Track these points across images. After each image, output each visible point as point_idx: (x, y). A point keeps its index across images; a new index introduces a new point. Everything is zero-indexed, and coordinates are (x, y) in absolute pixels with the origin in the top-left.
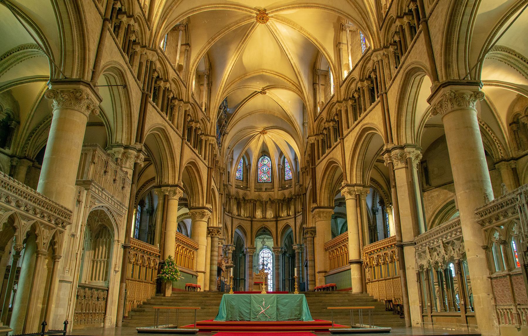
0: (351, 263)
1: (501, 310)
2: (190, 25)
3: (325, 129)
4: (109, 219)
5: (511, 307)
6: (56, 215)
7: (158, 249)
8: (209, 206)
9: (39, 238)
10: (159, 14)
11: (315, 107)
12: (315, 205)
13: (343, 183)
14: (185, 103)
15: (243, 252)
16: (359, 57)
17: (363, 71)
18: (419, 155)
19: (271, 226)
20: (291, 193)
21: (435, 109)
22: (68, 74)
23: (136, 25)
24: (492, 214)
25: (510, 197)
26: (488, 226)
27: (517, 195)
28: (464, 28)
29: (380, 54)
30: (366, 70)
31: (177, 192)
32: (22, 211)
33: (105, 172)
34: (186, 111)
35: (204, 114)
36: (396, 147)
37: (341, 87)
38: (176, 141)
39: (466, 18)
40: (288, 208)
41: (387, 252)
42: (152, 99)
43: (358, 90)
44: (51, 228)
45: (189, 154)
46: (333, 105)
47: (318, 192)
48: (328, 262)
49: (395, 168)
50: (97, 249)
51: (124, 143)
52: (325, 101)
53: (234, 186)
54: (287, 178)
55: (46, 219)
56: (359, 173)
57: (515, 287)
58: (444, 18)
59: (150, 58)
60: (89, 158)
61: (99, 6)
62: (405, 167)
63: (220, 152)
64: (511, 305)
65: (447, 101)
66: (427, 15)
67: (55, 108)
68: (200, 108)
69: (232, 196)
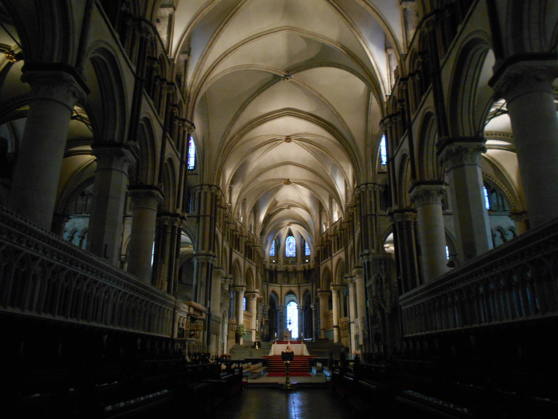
0: (334, 327)
12: (319, 290)
14: (245, 237)
15: (275, 308)
19: (295, 289)
34: (245, 241)
53: (268, 261)
69: (267, 270)
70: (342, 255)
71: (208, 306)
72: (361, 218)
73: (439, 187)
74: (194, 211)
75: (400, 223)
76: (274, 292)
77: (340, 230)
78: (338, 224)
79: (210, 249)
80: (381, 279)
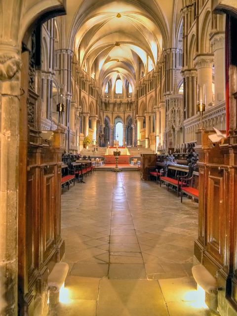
12: (137, 115)
19: (122, 115)
20: (131, 100)
70: (153, 94)
71: (68, 125)
72: (166, 71)
73: (211, 57)
74: (56, 66)
75: (188, 78)
76: (107, 116)
77: (153, 77)
78: (151, 73)
79: (68, 91)
80: (175, 111)
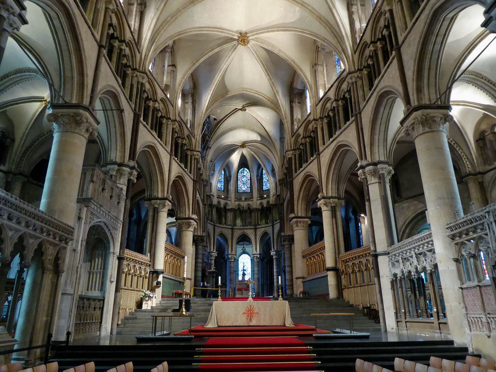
0: (328, 270)
1: (472, 319)
2: (175, 47)
3: (302, 144)
4: (105, 233)
5: (480, 316)
6: (60, 232)
7: (149, 259)
8: (195, 217)
9: (45, 254)
10: (148, 38)
11: (292, 123)
12: (292, 215)
13: (319, 196)
16: (335, 78)
17: (339, 91)
18: (391, 171)
20: (268, 202)
21: (407, 130)
22: (67, 99)
23: (127, 49)
24: (463, 229)
25: (478, 215)
26: (458, 240)
27: (485, 213)
28: (435, 56)
29: (354, 76)
30: (341, 90)
31: (166, 204)
32: (30, 231)
33: (103, 189)
34: (173, 129)
35: (189, 130)
36: (370, 164)
37: (317, 105)
38: (165, 156)
39: (437, 47)
40: (267, 218)
41: (361, 260)
42: (142, 118)
43: (333, 110)
44: (55, 245)
45: (176, 169)
46: (309, 122)
47: (295, 203)
48: (306, 268)
49: (369, 183)
50: (93, 261)
51: (118, 161)
52: (302, 118)
54: (265, 188)
55: (51, 237)
56: (334, 186)
57: (484, 298)
58: (416, 46)
59: (141, 80)
60: (88, 177)
61: (95, 33)
62: (378, 182)
63: (204, 166)
64: (481, 314)
65: (419, 124)
66: (400, 41)
67: (56, 131)
68: (186, 125)
76: (222, 235)
